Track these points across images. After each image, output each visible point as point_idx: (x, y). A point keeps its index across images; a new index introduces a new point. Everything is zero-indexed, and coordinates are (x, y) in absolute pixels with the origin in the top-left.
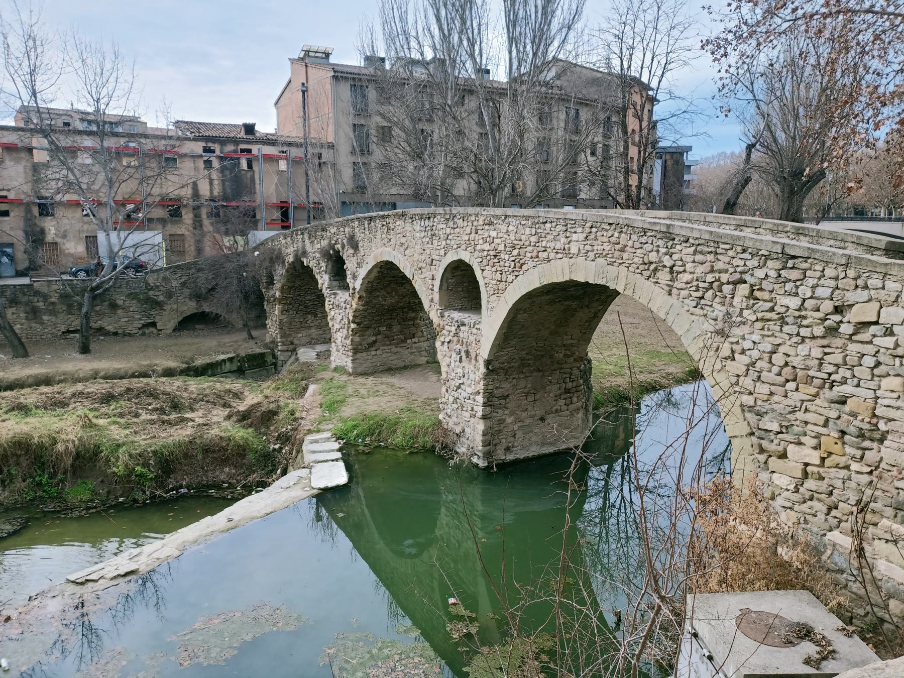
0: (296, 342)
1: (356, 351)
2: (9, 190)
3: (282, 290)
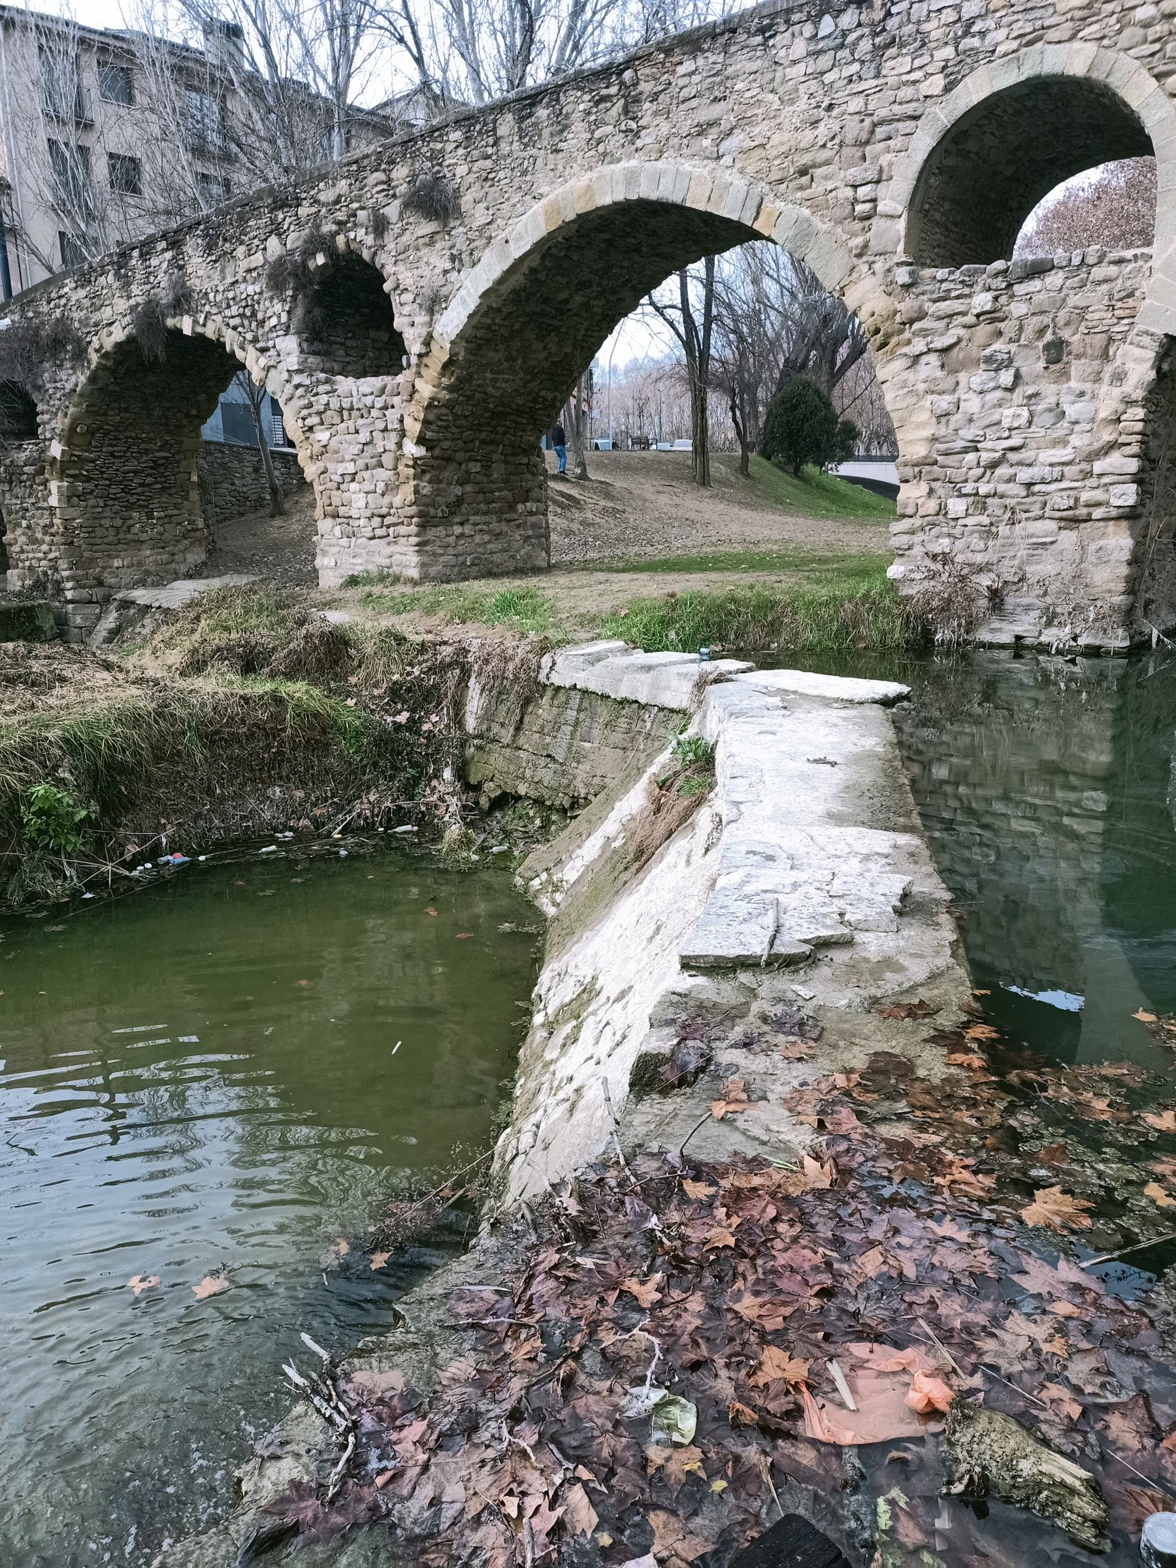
1: (426, 522)
3: (69, 437)
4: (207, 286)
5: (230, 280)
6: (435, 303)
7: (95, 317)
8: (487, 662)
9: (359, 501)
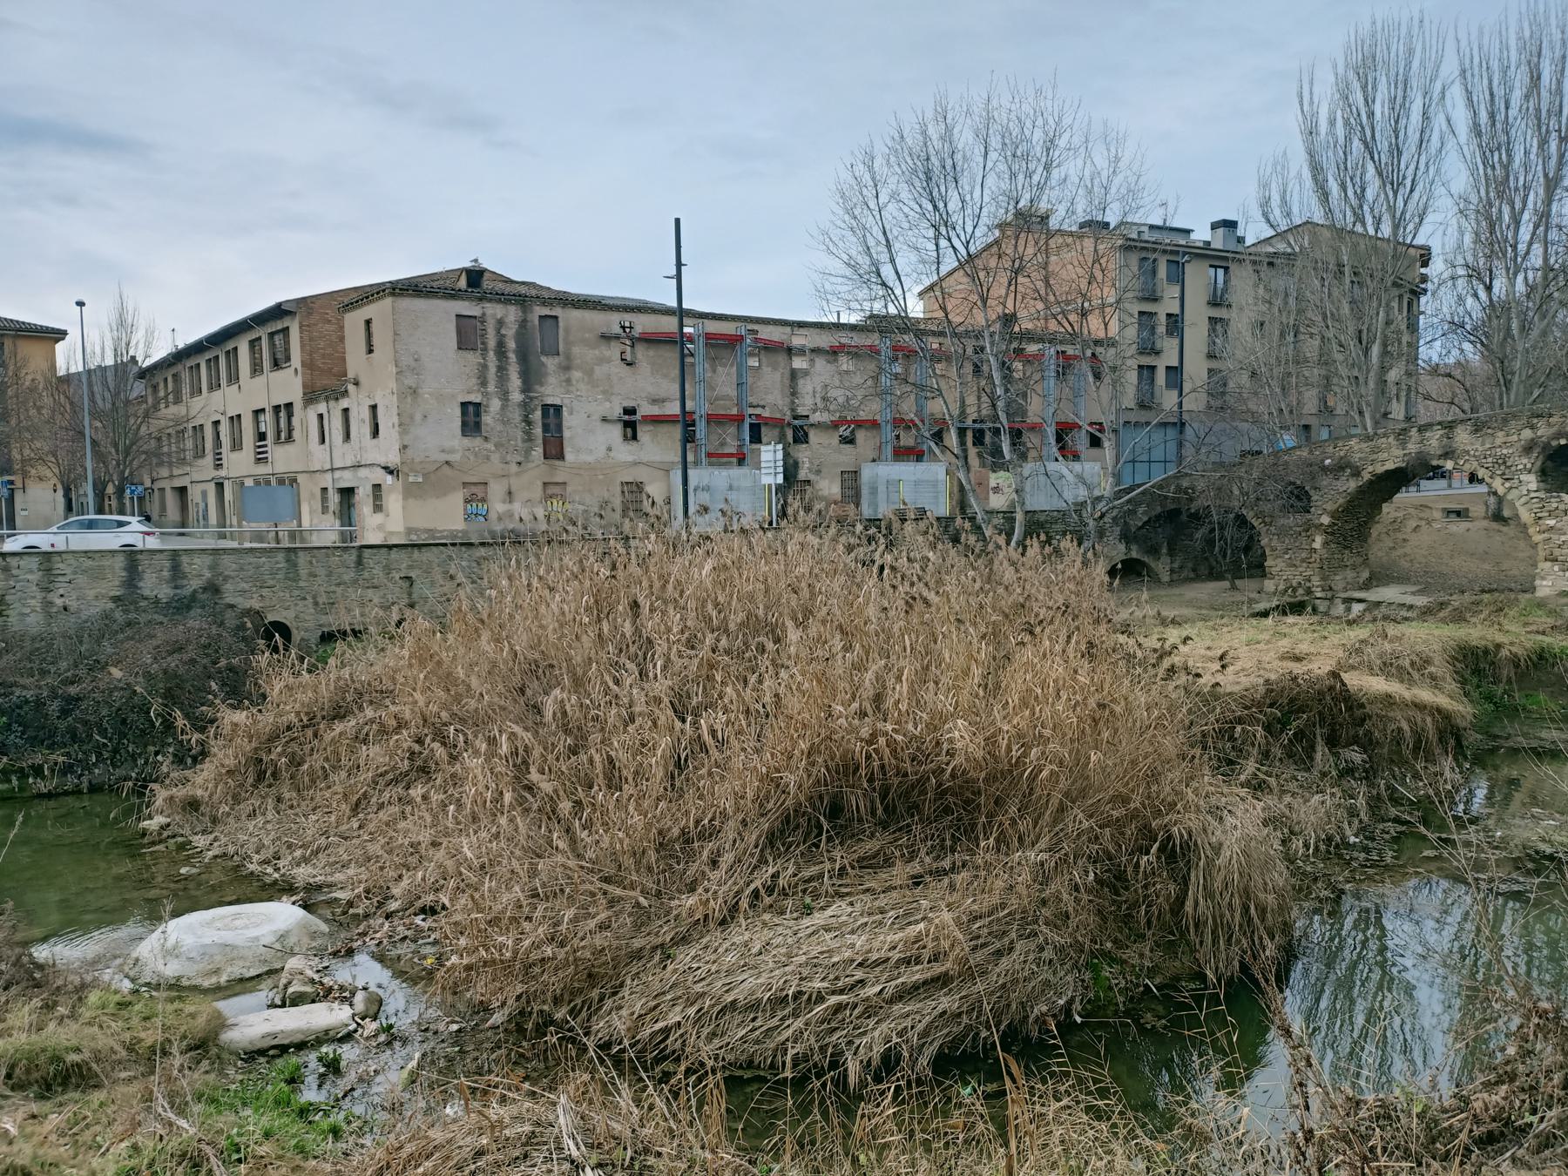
0: (1335, 588)
2: (763, 407)
7: (1375, 456)
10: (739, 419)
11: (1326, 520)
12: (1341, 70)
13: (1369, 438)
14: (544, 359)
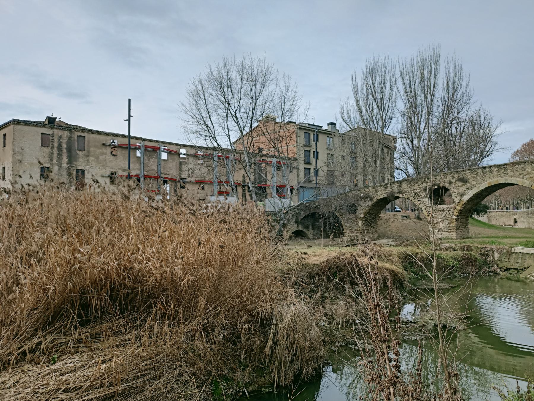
2: (168, 174)
3: (366, 214)
4: (406, 190)
5: (412, 189)
6: (462, 195)
7: (377, 193)
8: (498, 249)
9: (441, 226)
10: (156, 178)
11: (362, 216)
12: (365, 73)
13: (375, 187)
14: (78, 152)
